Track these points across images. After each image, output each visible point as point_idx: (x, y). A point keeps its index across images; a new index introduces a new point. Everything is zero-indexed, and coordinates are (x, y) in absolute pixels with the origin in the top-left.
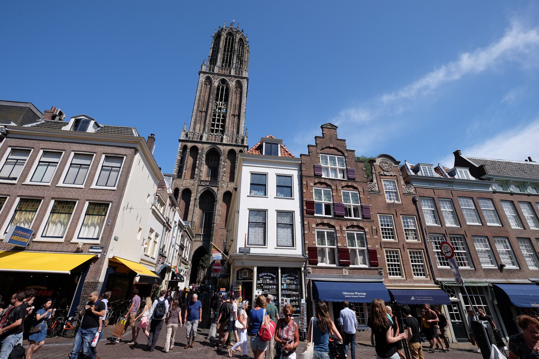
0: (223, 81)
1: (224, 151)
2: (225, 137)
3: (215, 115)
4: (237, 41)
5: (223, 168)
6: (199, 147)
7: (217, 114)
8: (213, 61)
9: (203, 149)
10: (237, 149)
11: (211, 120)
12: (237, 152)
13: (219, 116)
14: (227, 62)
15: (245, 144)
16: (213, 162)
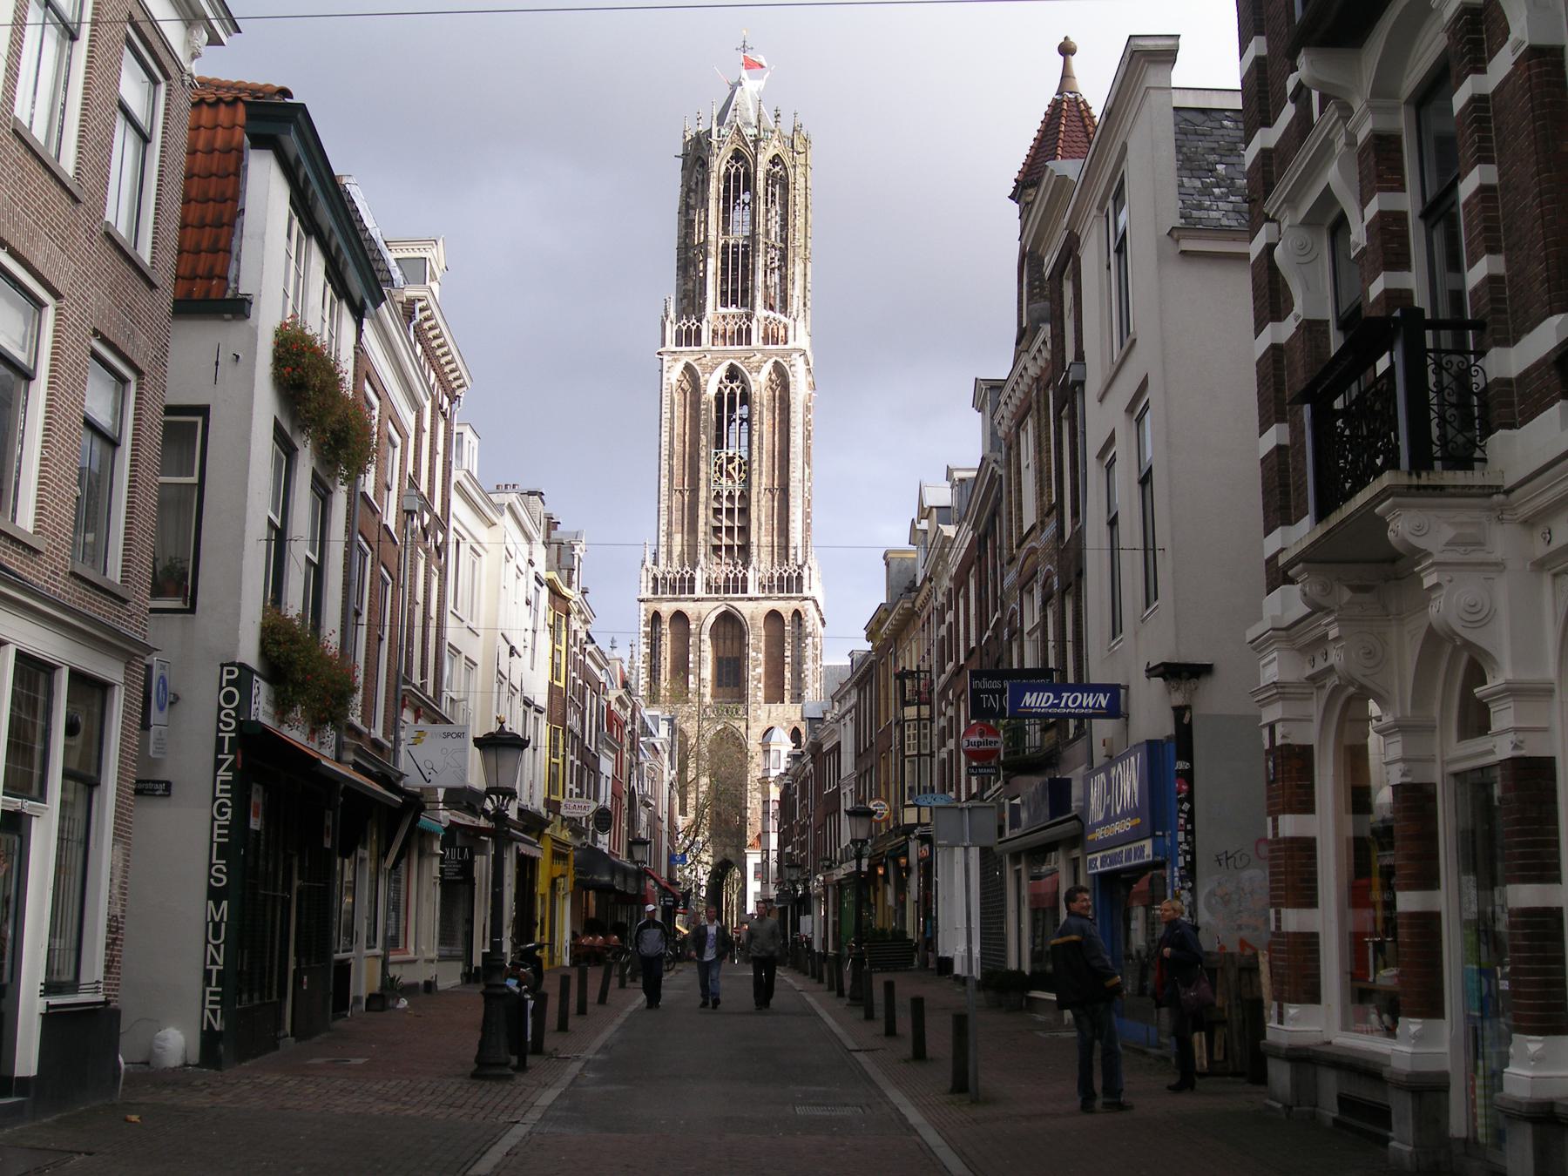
0: (733, 374)
1: (752, 618)
2: (750, 575)
3: (718, 496)
4: (761, 185)
5: (755, 668)
6: (689, 614)
7: (725, 494)
8: (691, 302)
9: (699, 618)
10: (785, 608)
11: (711, 513)
12: (787, 617)
13: (730, 497)
14: (738, 292)
15: (806, 593)
16: (728, 642)
